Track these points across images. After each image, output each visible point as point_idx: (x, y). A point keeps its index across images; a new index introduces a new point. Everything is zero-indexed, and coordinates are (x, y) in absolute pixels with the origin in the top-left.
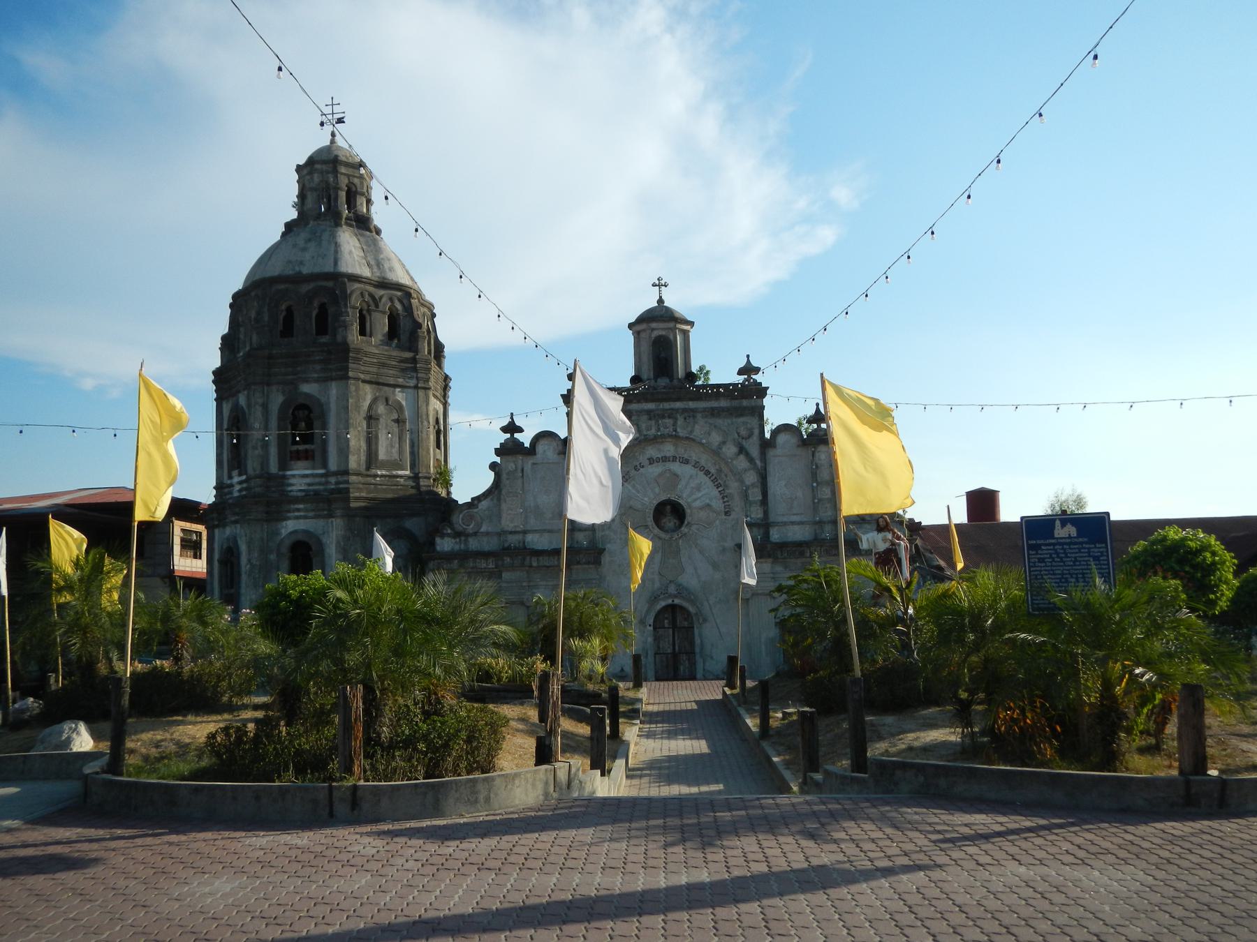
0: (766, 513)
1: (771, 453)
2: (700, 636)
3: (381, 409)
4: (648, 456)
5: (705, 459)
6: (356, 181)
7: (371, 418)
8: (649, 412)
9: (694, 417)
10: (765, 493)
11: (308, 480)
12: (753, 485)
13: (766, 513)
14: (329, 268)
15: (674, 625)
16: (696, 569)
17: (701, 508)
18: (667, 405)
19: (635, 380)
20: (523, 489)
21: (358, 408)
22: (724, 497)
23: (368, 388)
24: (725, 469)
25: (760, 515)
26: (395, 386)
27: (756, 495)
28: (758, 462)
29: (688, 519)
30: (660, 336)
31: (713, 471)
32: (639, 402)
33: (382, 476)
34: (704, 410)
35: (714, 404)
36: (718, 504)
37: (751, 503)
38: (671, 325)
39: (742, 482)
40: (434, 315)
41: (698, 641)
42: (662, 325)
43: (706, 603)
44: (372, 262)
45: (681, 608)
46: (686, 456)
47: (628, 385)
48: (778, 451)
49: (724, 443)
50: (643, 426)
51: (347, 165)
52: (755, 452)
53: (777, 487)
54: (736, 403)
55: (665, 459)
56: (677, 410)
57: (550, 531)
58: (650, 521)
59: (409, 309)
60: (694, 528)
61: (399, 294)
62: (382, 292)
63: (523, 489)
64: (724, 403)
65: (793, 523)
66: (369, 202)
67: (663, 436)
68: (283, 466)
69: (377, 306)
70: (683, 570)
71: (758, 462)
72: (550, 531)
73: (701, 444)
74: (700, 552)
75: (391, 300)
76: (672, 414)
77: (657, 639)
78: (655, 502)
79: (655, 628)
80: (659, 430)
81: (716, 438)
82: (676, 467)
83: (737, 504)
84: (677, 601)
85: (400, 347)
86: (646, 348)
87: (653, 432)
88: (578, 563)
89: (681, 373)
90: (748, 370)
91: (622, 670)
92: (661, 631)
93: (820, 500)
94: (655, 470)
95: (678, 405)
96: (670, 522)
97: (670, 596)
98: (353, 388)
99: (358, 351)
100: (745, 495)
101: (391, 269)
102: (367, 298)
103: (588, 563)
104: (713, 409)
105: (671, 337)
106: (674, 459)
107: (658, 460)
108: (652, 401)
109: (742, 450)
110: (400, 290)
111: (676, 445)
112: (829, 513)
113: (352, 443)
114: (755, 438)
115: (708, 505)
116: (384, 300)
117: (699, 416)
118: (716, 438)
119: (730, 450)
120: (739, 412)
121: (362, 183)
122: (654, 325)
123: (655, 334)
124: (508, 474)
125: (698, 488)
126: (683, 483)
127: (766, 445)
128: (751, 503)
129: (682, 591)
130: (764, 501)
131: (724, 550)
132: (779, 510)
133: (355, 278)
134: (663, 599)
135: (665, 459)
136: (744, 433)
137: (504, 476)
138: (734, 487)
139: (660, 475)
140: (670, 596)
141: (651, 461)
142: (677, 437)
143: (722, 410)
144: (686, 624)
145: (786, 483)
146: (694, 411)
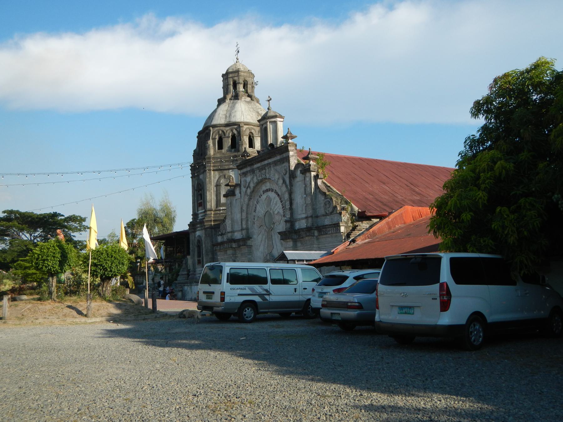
0: (292, 214)
3: (222, 181)
6: (236, 78)
7: (218, 186)
8: (258, 168)
10: (291, 204)
11: (202, 215)
13: (292, 214)
14: (209, 124)
20: (231, 212)
21: (210, 182)
23: (217, 173)
26: (229, 169)
33: (223, 210)
36: (281, 211)
38: (265, 121)
44: (228, 116)
50: (258, 175)
51: (232, 73)
55: (267, 190)
59: (239, 133)
61: (236, 127)
62: (228, 128)
63: (231, 212)
65: (302, 219)
66: (245, 85)
68: (198, 211)
69: (225, 135)
75: (232, 131)
81: (277, 176)
85: (235, 151)
95: (266, 162)
98: (208, 174)
99: (210, 158)
101: (235, 116)
102: (221, 132)
104: (275, 161)
109: (284, 182)
110: (236, 125)
113: (208, 198)
114: (288, 175)
116: (228, 132)
117: (272, 166)
119: (281, 181)
121: (239, 78)
125: (276, 204)
130: (291, 209)
133: (214, 126)
135: (267, 190)
136: (284, 172)
142: (266, 178)
146: (269, 164)
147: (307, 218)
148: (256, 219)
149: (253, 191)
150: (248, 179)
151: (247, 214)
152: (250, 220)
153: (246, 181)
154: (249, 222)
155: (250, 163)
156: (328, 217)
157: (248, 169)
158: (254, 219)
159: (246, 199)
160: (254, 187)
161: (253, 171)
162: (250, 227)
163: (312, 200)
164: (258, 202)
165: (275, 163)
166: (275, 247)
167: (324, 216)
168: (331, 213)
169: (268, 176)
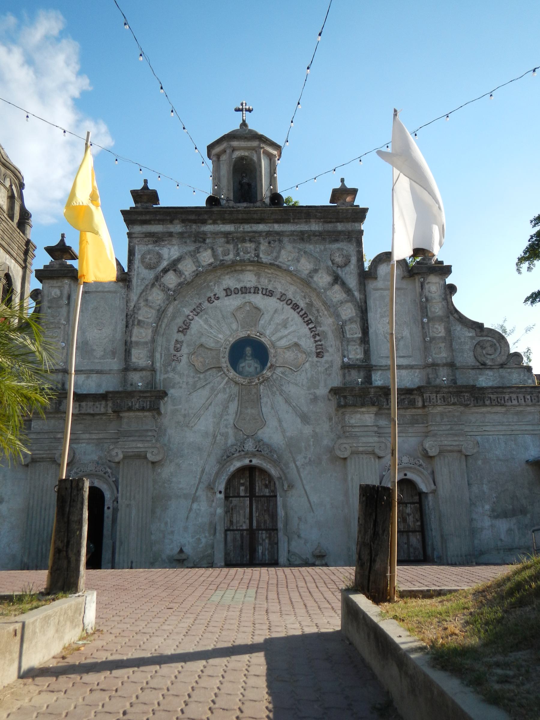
1: (371, 285)
2: (285, 506)
4: (225, 287)
5: (292, 291)
8: (226, 235)
9: (280, 241)
10: (365, 330)
12: (351, 320)
13: (367, 352)
15: (252, 495)
16: (280, 421)
17: (288, 348)
18: (247, 227)
19: (212, 201)
22: (315, 334)
24: (317, 303)
25: (360, 356)
27: (354, 331)
28: (357, 294)
29: (272, 360)
30: (242, 158)
31: (302, 304)
32: (215, 222)
34: (292, 233)
35: (303, 227)
36: (308, 344)
37: (349, 341)
38: (255, 144)
39: (337, 316)
40: (22, 186)
41: (281, 512)
42: (243, 144)
43: (292, 465)
45: (263, 471)
46: (270, 287)
47: (203, 204)
48: (379, 284)
49: (316, 271)
50: (220, 250)
52: (352, 282)
53: (378, 325)
54: (329, 227)
55: (244, 290)
56: (260, 233)
57: (98, 372)
58: (225, 362)
60: (279, 371)
64: (315, 227)
67: (242, 261)
70: (264, 423)
71: (357, 294)
72: (98, 372)
73: (287, 271)
74: (287, 401)
76: (253, 237)
77: (229, 511)
78: (232, 340)
79: (227, 497)
80: (238, 254)
82: (258, 300)
83: (331, 342)
84: (255, 462)
86: (225, 170)
87: (231, 256)
88: (130, 409)
89: (265, 192)
90: (342, 193)
91: (181, 551)
92: (235, 501)
93: (433, 339)
94: (234, 302)
95: (261, 227)
96: (249, 365)
97: (247, 454)
100: (341, 331)
103: (143, 409)
104: (302, 233)
105: (255, 158)
106: (256, 290)
107: (237, 291)
108: (232, 221)
109: (337, 279)
111: (258, 275)
112: (444, 355)
115: (296, 345)
117: (285, 240)
118: (305, 266)
119: (323, 279)
120: (335, 237)
122: (235, 143)
123: (237, 154)
124: (50, 301)
125: (285, 324)
126: (267, 317)
127: (366, 276)
128: (349, 341)
129: (262, 449)
131: (315, 399)
132: (380, 352)
134: (240, 458)
135: (244, 290)
137: (45, 304)
138: (327, 324)
139: (240, 308)
140: (247, 454)
141: (228, 292)
143: (314, 234)
144: (267, 492)
145: (391, 317)
146: (280, 234)
147: (434, 365)
148: (185, 350)
149: (188, 284)
150: (170, 252)
151: (156, 332)
152: (159, 349)
153: (160, 257)
154: (158, 355)
155: (193, 217)
156: (490, 373)
157: (177, 228)
158: (177, 350)
159: (157, 297)
160: (197, 275)
161: (200, 239)
162: (158, 365)
163: (449, 331)
164: (198, 311)
165: (303, 237)
166: (272, 423)
167: (473, 368)
168: (502, 366)
169: (265, 258)
